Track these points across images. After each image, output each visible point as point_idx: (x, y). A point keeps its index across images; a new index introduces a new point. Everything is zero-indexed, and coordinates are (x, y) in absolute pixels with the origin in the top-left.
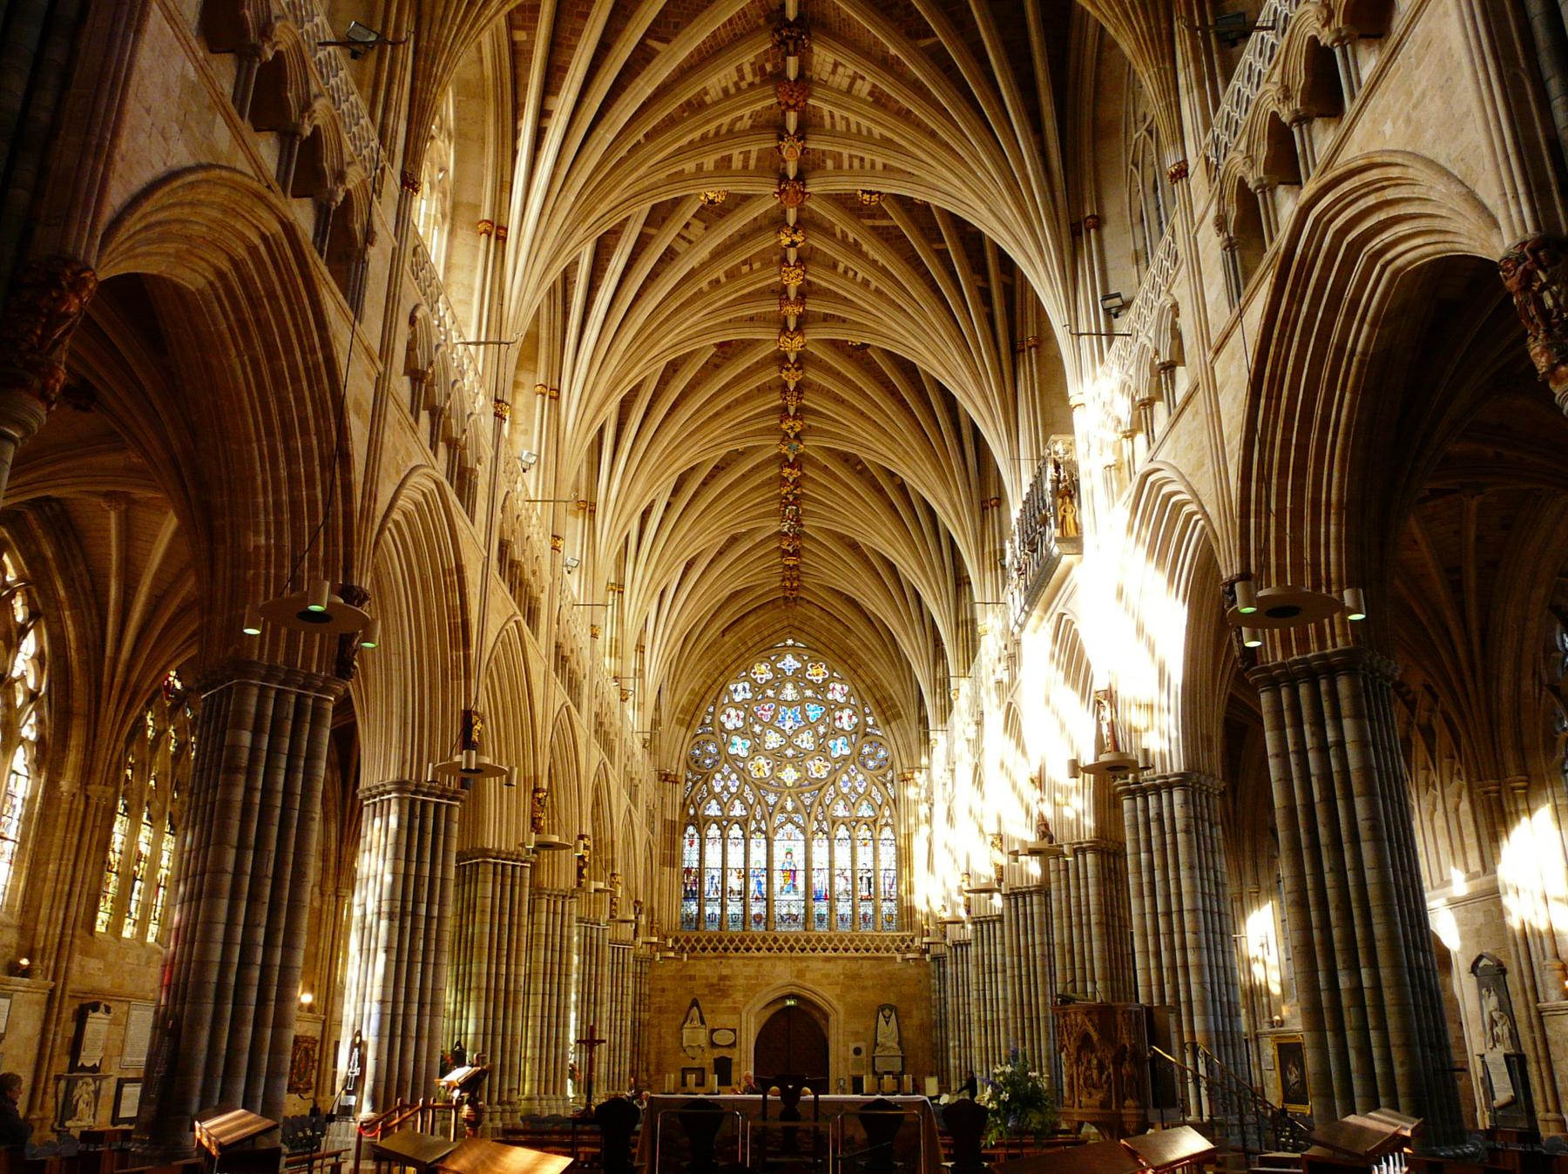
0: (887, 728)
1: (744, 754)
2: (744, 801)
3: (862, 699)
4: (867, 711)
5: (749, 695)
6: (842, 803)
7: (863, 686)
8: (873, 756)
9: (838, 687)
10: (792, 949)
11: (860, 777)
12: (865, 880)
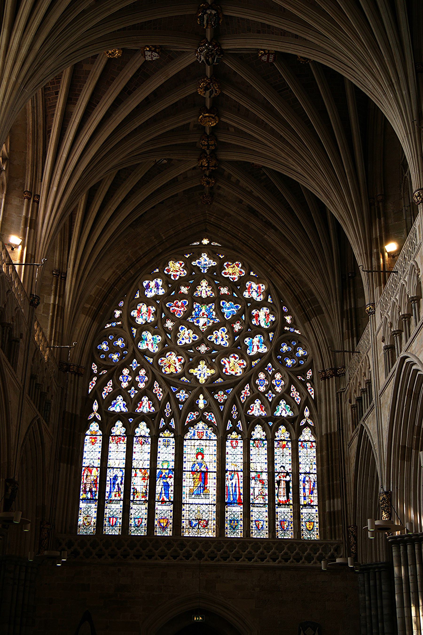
0: (307, 325)
1: (154, 349)
2: (152, 398)
3: (280, 298)
4: (285, 309)
5: (161, 292)
6: (258, 402)
7: (281, 283)
8: (291, 355)
9: (255, 286)
10: (200, 556)
11: (278, 376)
12: (283, 485)
